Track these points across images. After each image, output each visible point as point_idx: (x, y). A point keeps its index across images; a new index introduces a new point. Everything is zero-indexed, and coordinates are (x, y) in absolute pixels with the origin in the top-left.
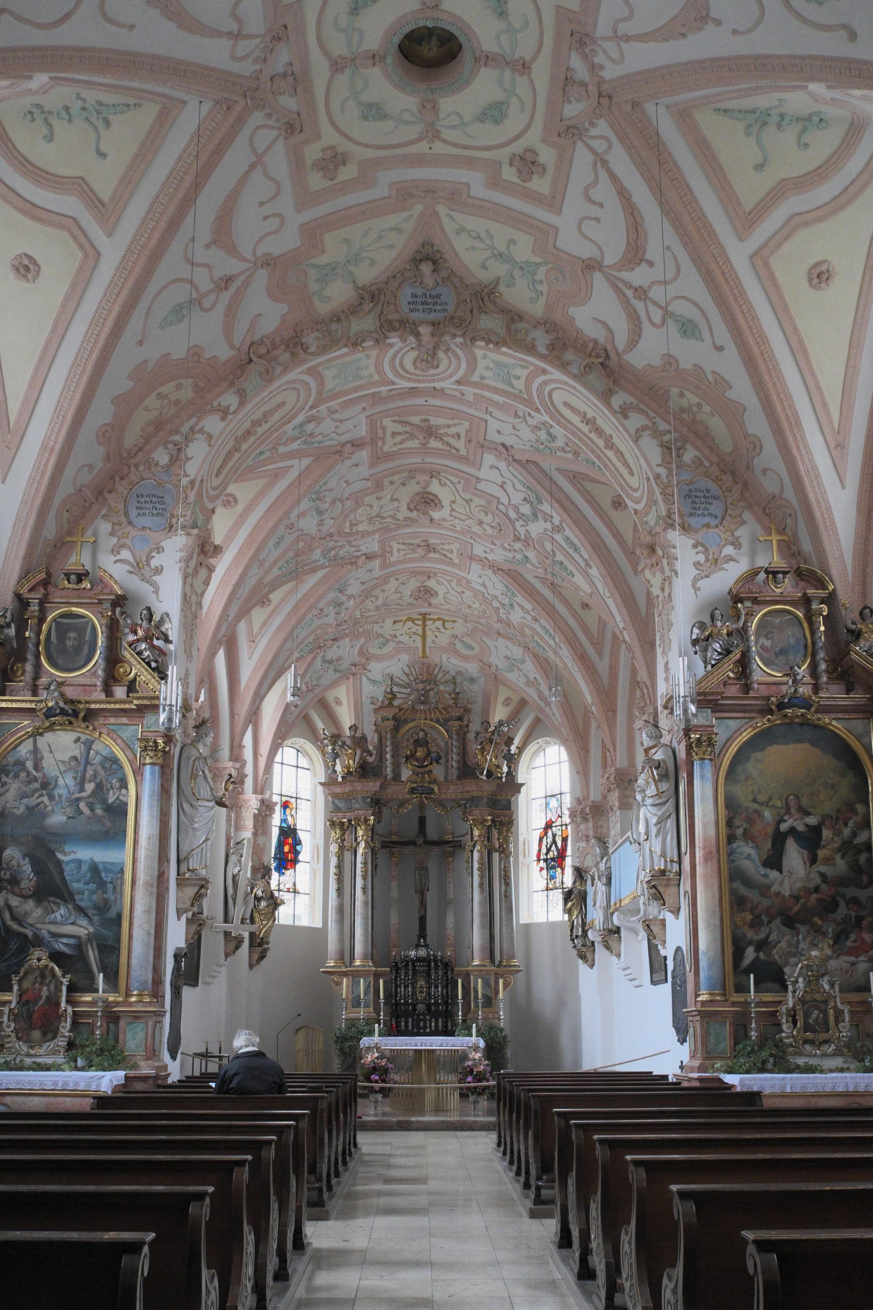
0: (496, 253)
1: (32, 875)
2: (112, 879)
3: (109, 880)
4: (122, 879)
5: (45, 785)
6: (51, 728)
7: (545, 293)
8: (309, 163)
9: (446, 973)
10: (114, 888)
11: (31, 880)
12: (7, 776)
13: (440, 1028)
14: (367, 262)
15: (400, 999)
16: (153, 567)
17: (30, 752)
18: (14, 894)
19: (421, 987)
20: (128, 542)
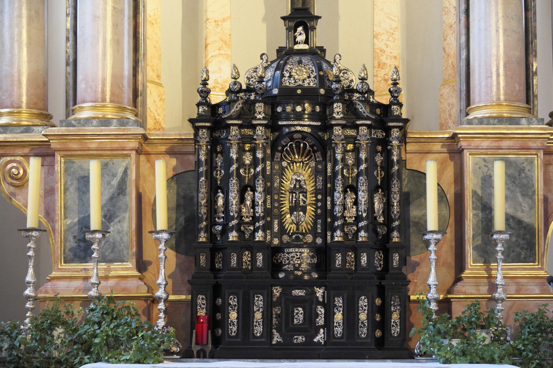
9: (385, 142)
13: (363, 332)
15: (225, 232)
19: (299, 188)
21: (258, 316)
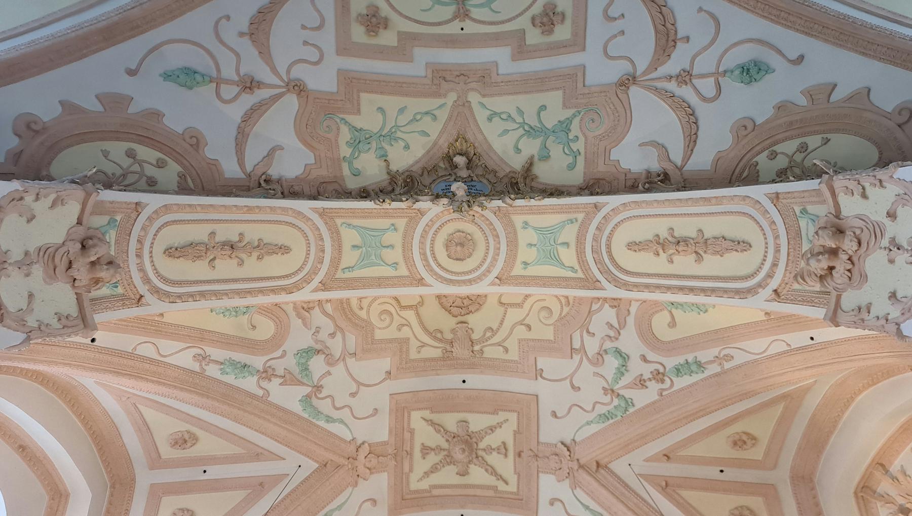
0: (527, 128)
7: (582, 151)
8: (354, 14)
14: (402, 144)
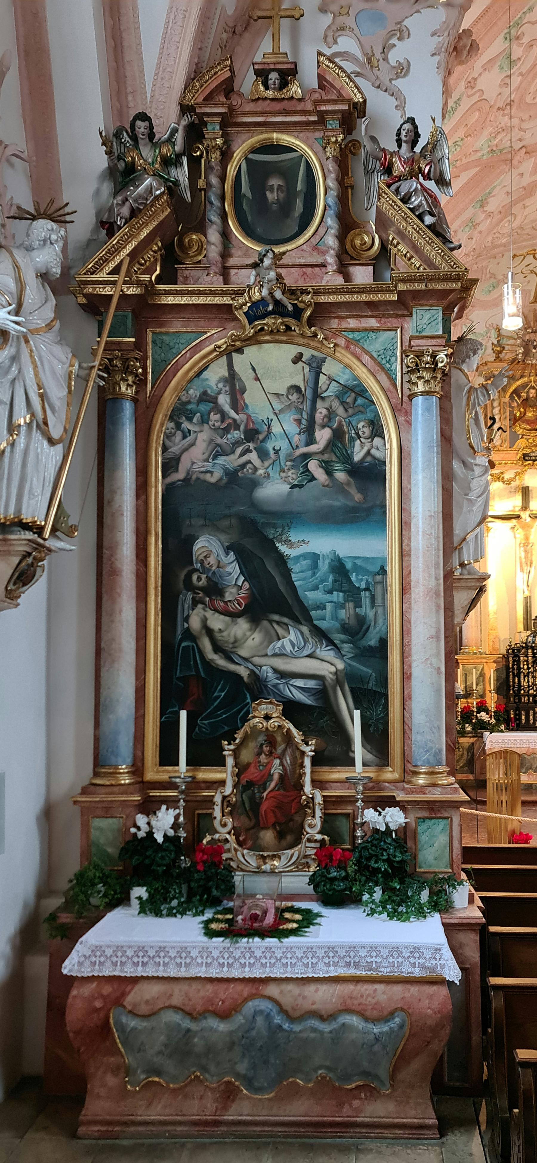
1: (242, 578)
2: (368, 583)
3: (363, 585)
4: (383, 583)
5: (251, 434)
6: (254, 340)
10: (373, 598)
11: (240, 588)
12: (190, 419)
16: (393, 62)
17: (225, 380)
18: (216, 610)
20: (350, 21)
21: (531, 717)
